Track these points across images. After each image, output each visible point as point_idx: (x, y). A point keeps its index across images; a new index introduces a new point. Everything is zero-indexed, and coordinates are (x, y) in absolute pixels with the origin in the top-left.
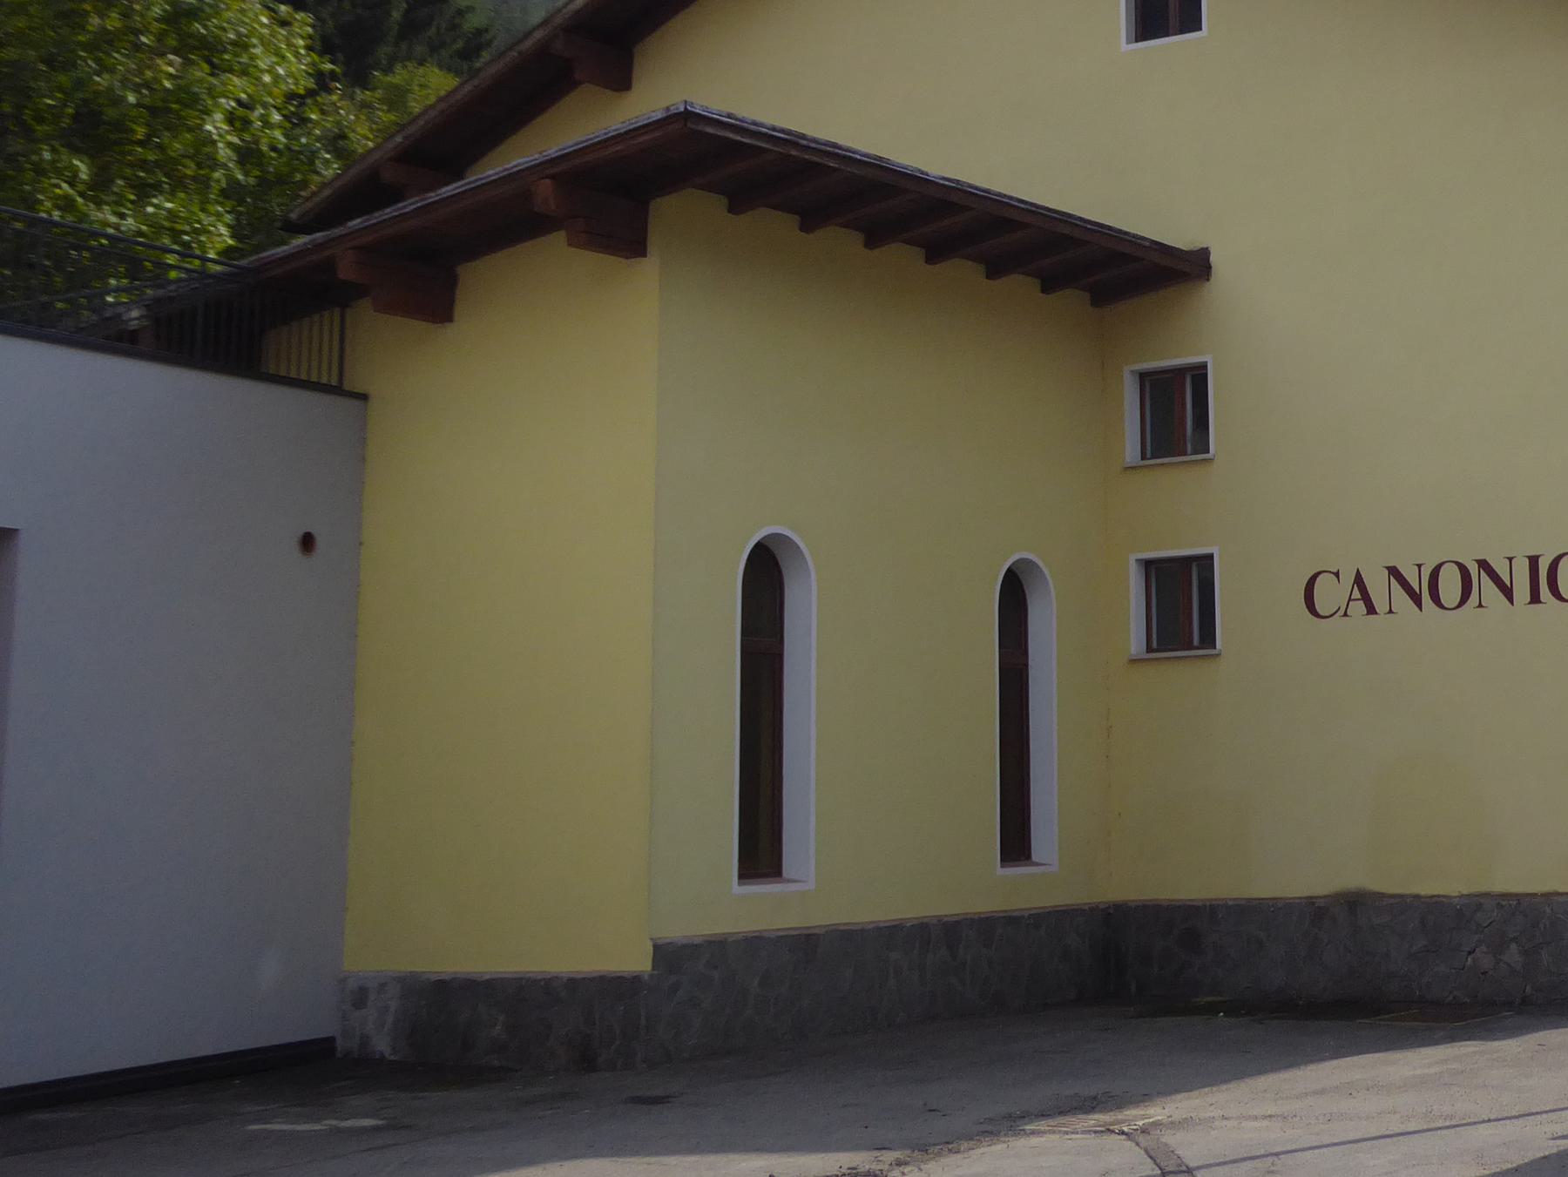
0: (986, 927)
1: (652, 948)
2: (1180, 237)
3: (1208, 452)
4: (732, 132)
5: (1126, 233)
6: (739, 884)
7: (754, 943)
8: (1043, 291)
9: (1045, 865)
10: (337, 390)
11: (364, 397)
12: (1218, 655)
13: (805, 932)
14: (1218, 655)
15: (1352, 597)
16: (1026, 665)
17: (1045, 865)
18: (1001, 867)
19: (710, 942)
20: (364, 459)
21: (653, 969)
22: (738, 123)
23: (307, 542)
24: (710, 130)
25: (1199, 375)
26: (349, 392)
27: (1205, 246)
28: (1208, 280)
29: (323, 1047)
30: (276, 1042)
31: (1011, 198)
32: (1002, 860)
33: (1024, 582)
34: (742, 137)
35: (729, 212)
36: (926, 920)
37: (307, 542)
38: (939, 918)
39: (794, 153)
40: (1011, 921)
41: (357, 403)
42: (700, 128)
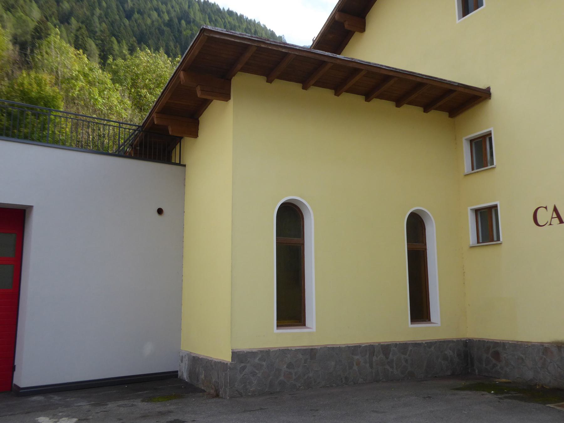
0: (403, 347)
1: (231, 353)
2: (481, 85)
3: (493, 165)
4: (230, 37)
5: (445, 80)
6: (277, 329)
7: (284, 352)
8: (424, 112)
9: (436, 323)
10: (179, 164)
11: (185, 166)
12: (501, 244)
13: (311, 348)
14: (501, 244)
15: (73, 120)
16: (426, 249)
17: (436, 323)
18: (411, 324)
19: (261, 351)
20: (185, 185)
21: (232, 361)
22: (232, 34)
23: (160, 211)
24: (217, 36)
25: (488, 136)
26: (182, 165)
27: (489, 86)
28: (490, 99)
29: (173, 375)
30: (152, 373)
31: (378, 65)
32: (411, 321)
33: (422, 217)
34: (235, 39)
35: (267, 82)
36: (372, 344)
37: (160, 211)
38: (379, 344)
39: (263, 46)
40: (417, 345)
41: (184, 167)
42: (211, 35)
